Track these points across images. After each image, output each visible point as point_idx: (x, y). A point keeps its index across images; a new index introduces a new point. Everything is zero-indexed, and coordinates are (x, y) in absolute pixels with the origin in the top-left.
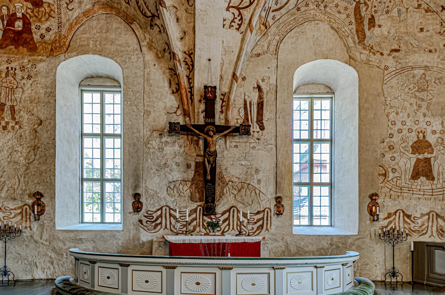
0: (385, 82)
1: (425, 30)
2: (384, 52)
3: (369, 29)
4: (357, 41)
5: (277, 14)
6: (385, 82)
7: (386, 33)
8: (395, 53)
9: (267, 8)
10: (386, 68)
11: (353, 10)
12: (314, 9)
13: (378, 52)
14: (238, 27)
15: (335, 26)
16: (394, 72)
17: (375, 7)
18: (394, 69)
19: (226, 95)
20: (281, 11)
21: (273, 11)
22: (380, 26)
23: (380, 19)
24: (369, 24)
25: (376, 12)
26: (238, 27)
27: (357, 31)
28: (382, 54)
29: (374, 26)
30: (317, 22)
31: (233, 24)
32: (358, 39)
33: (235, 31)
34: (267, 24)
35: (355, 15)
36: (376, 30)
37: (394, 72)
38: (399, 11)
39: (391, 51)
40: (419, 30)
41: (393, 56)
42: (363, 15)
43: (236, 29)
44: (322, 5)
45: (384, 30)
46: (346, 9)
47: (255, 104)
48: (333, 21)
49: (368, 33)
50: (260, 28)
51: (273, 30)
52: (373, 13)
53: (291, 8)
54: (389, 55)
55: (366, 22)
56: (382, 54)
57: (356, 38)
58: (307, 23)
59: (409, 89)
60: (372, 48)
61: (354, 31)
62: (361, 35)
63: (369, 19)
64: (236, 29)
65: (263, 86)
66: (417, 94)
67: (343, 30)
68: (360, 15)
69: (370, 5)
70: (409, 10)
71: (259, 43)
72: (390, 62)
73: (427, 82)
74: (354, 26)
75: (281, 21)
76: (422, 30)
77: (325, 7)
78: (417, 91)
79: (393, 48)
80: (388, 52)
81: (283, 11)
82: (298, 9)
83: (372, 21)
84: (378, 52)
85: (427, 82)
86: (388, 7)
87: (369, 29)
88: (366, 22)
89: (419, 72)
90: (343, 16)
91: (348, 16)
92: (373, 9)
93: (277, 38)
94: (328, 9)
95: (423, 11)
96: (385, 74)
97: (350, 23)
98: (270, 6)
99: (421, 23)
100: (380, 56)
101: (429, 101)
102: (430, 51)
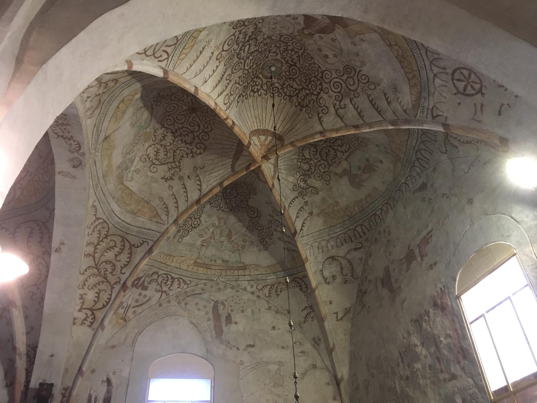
0: (241, 377)
1: (277, 329)
2: (241, 348)
3: (226, 325)
4: (215, 336)
5: (139, 310)
6: (241, 377)
7: (242, 329)
8: (250, 349)
9: (126, 306)
10: (242, 363)
11: (211, 309)
12: (175, 306)
13: (234, 346)
14: (90, 324)
15: (193, 321)
16: (249, 367)
17: (231, 306)
18: (249, 364)
19: (69, 390)
20: (143, 306)
21: (133, 307)
22: (236, 323)
23: (236, 317)
24: (226, 321)
25: (232, 311)
26: (90, 324)
27: (215, 327)
28: (238, 349)
29: (231, 323)
30: (177, 317)
31: (85, 322)
32: (216, 334)
33: (86, 328)
34: (126, 318)
35: (213, 313)
36: (233, 327)
37: (249, 367)
38: (253, 311)
39: (246, 347)
40: (272, 328)
41: (248, 351)
42: (220, 312)
43: (88, 326)
44: (183, 303)
45: (240, 327)
46: (205, 307)
47: (101, 400)
48: (193, 317)
49: (225, 329)
50: (117, 322)
51: (131, 323)
52: (230, 312)
53: (153, 303)
54: (244, 350)
55: (223, 319)
56: (238, 349)
57: (214, 333)
58: (167, 318)
59: (265, 384)
60: (229, 343)
61: (212, 327)
62: (219, 332)
63: (226, 316)
64: (88, 326)
65: (114, 380)
66: (273, 389)
67: (202, 325)
68: (218, 313)
69: (227, 305)
70: (261, 311)
71: (115, 336)
72: (245, 357)
73: (282, 378)
74: (212, 323)
75: (142, 314)
76: (274, 328)
77: (186, 304)
78: (273, 386)
79: (249, 343)
80: (244, 347)
81: (145, 307)
82: (160, 305)
83: (229, 319)
84: (234, 346)
85: (282, 378)
86: (243, 307)
87: (226, 325)
88: (223, 319)
89: (273, 368)
90: (202, 313)
91: (207, 313)
92: (230, 308)
93: (136, 330)
94: (188, 306)
95: (274, 313)
96: (241, 369)
97: (209, 320)
98: (129, 304)
99: (273, 322)
100: (236, 351)
101: (286, 398)
102: (283, 348)
